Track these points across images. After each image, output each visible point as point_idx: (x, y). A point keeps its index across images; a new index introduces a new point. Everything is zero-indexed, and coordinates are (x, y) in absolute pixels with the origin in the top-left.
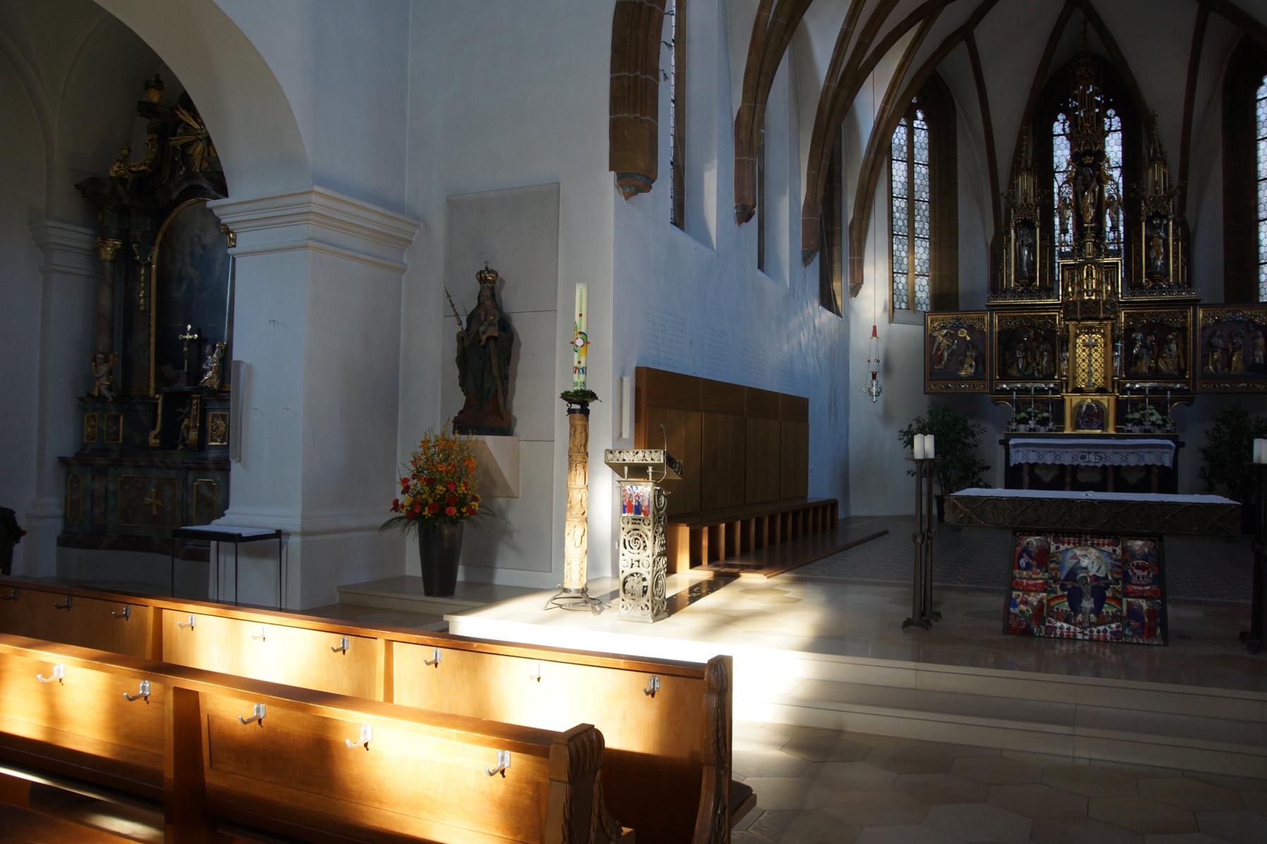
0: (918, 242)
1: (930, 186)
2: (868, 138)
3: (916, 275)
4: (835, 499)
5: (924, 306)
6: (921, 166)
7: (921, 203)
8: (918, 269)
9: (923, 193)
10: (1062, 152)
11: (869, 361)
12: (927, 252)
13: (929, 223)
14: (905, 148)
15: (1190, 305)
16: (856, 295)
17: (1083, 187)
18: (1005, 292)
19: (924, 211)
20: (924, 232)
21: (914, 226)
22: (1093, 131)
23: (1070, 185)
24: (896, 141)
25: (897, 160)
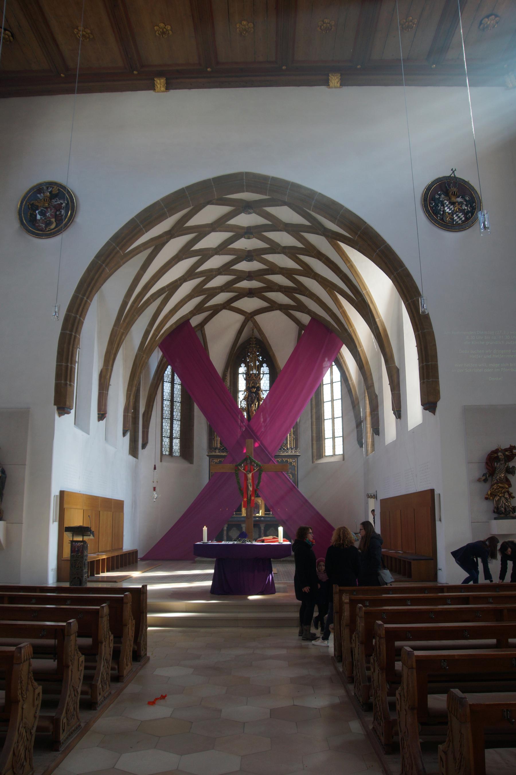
0: (175, 422)
1: (182, 395)
2: (154, 373)
3: (174, 438)
4: (136, 549)
5: (177, 453)
6: (178, 385)
7: (177, 403)
8: (174, 435)
9: (178, 397)
10: (242, 384)
11: (153, 482)
12: (179, 426)
13: (181, 413)
14: (170, 376)
15: (295, 458)
16: (144, 449)
17: (251, 402)
18: (216, 449)
19: (178, 407)
20: (178, 417)
21: (173, 414)
22: (256, 378)
23: (245, 401)
24: (166, 372)
25: (166, 382)
